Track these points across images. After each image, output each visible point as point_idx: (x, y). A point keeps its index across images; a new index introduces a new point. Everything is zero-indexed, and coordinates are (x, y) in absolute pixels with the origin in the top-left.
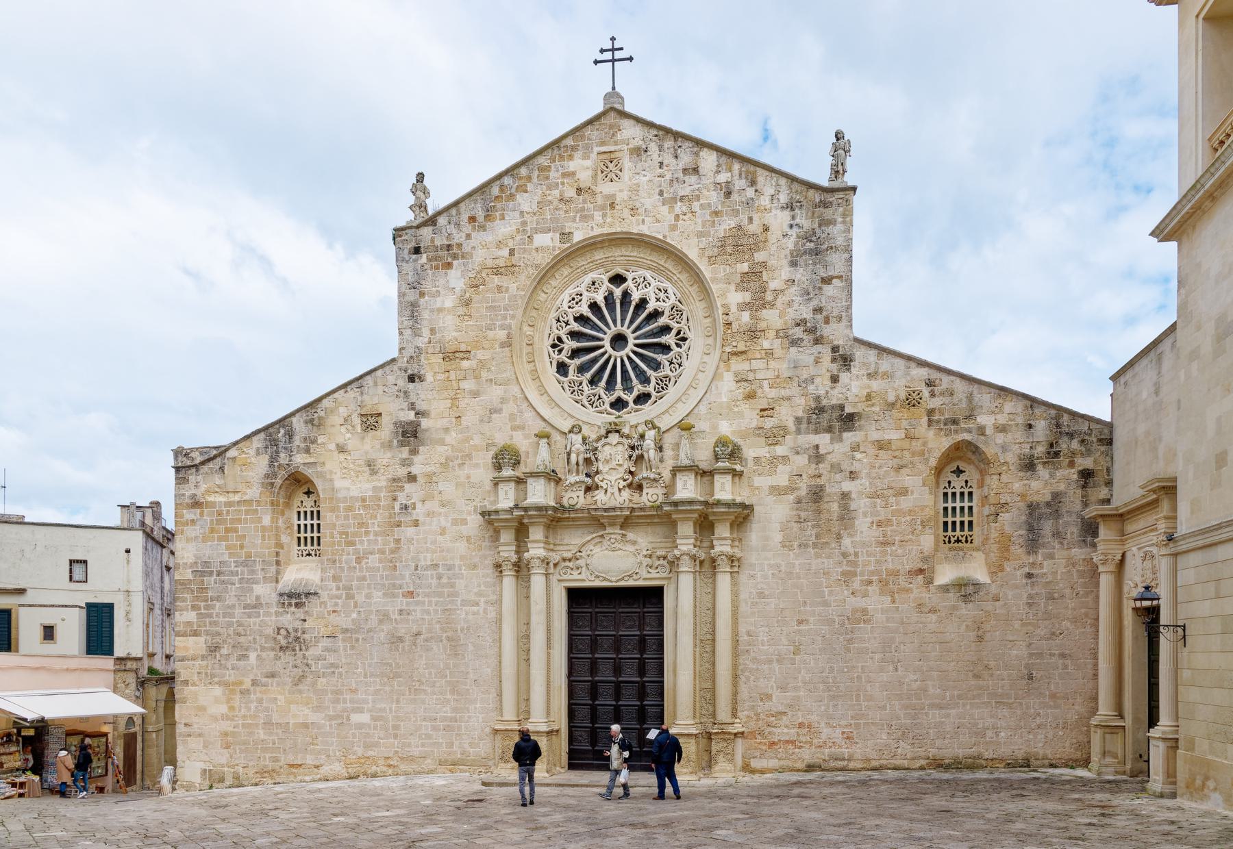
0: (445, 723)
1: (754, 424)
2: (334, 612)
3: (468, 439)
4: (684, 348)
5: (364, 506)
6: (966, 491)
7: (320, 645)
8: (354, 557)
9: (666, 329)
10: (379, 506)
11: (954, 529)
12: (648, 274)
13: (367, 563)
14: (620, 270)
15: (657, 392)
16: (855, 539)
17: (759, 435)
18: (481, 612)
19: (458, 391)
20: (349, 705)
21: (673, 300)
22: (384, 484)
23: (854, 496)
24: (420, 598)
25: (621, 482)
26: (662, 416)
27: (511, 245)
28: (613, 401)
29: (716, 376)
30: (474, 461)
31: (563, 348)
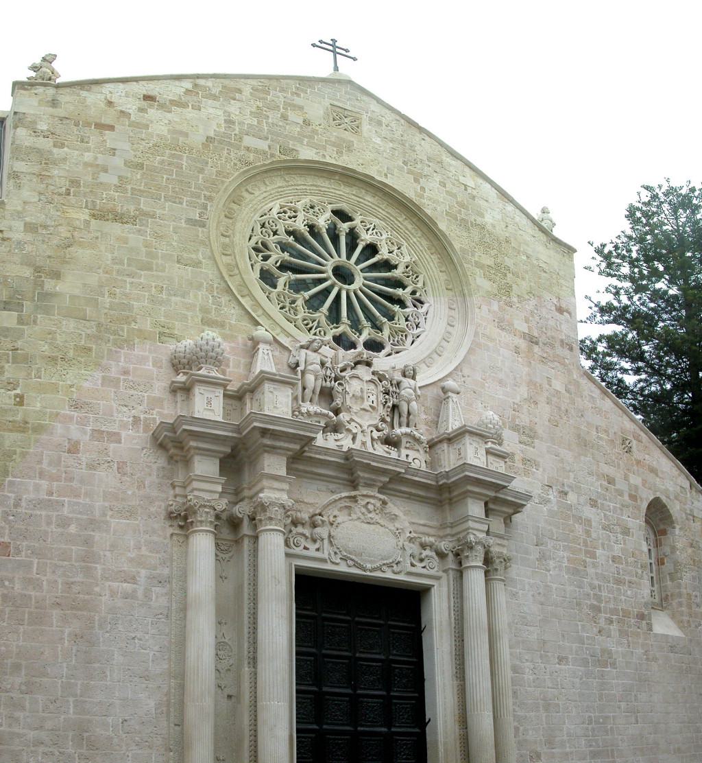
18: (140, 594)
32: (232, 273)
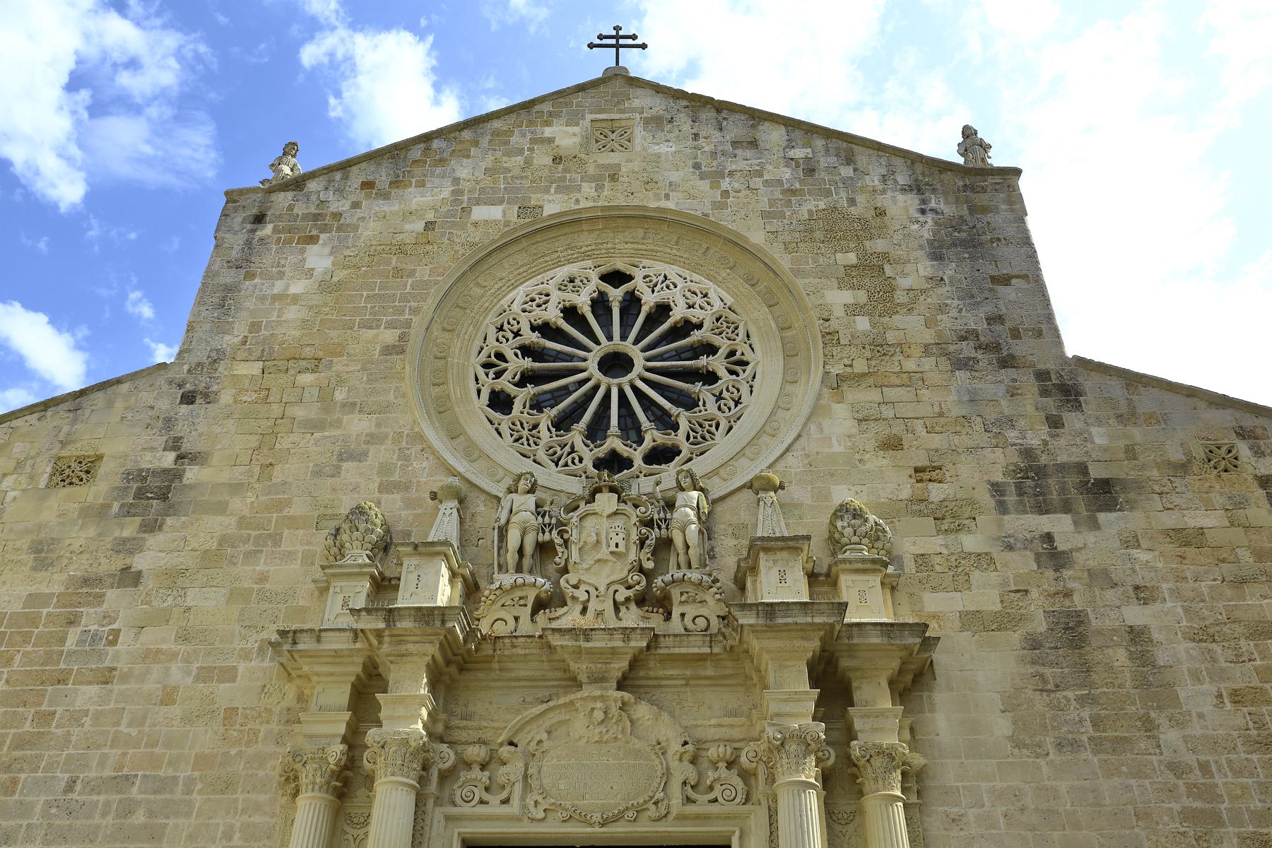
1: (906, 493)
3: (280, 505)
12: (672, 271)
14: (621, 265)
15: (691, 444)
16: (1188, 732)
17: (920, 513)
19: (279, 421)
21: (717, 305)
22: (57, 589)
23: (1156, 636)
25: (622, 589)
27: (430, 216)
29: (817, 411)
30: (285, 547)
31: (505, 370)
32: (442, 409)
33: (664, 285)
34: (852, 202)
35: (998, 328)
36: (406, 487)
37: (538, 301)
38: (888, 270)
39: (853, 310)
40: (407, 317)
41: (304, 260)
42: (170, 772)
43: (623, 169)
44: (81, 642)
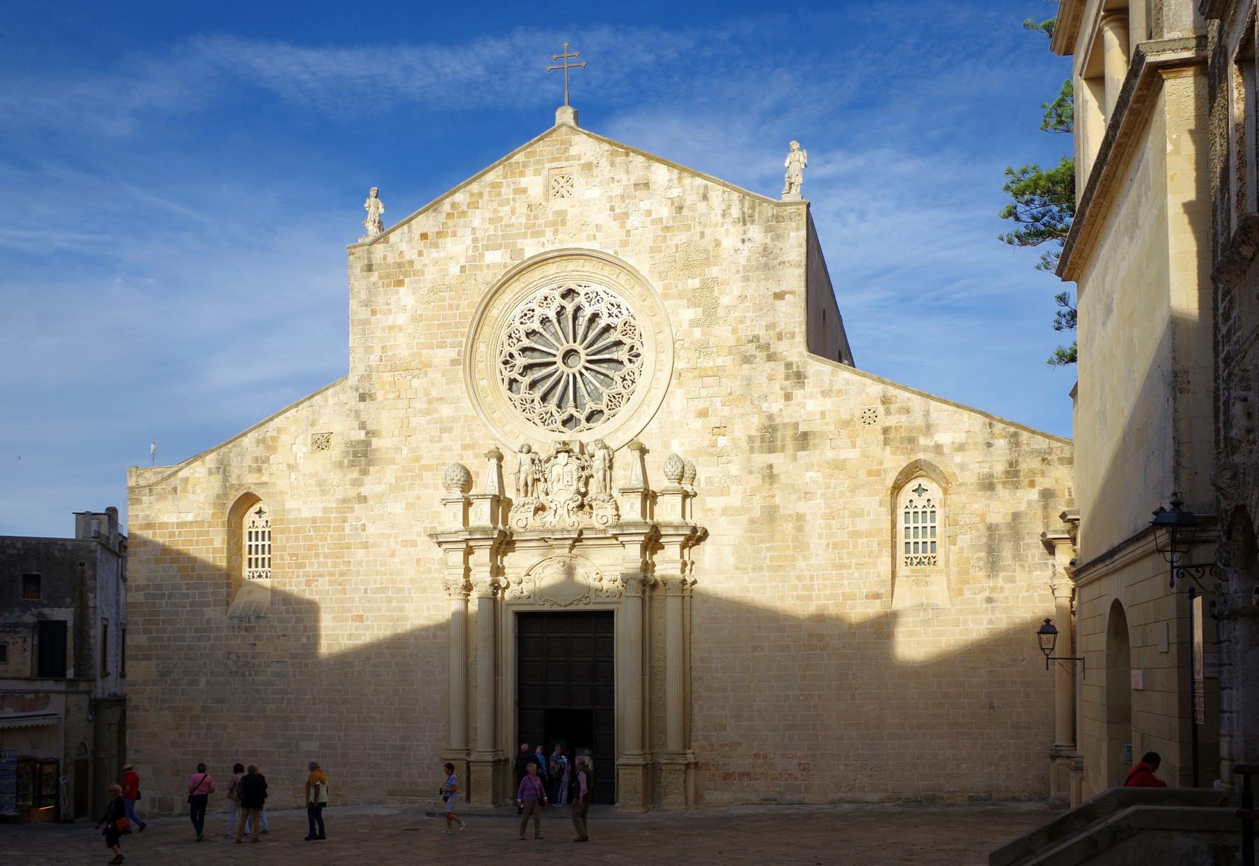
0: (393, 752)
2: (284, 636)
4: (637, 364)
5: (315, 527)
6: (929, 510)
7: (269, 670)
8: (304, 580)
9: (619, 343)
10: (329, 527)
11: (916, 551)
13: (317, 586)
15: (610, 410)
16: (809, 562)
19: (408, 410)
20: (297, 732)
22: (334, 505)
23: (808, 517)
24: (369, 623)
25: (570, 502)
26: (613, 434)
27: (462, 262)
28: (565, 418)
31: (515, 364)
33: (597, 299)
34: (702, 234)
35: (771, 333)
36: (474, 448)
37: (528, 316)
38: (716, 293)
39: (694, 323)
40: (460, 339)
41: (399, 299)
42: (401, 586)
43: (569, 214)
44: (351, 530)
